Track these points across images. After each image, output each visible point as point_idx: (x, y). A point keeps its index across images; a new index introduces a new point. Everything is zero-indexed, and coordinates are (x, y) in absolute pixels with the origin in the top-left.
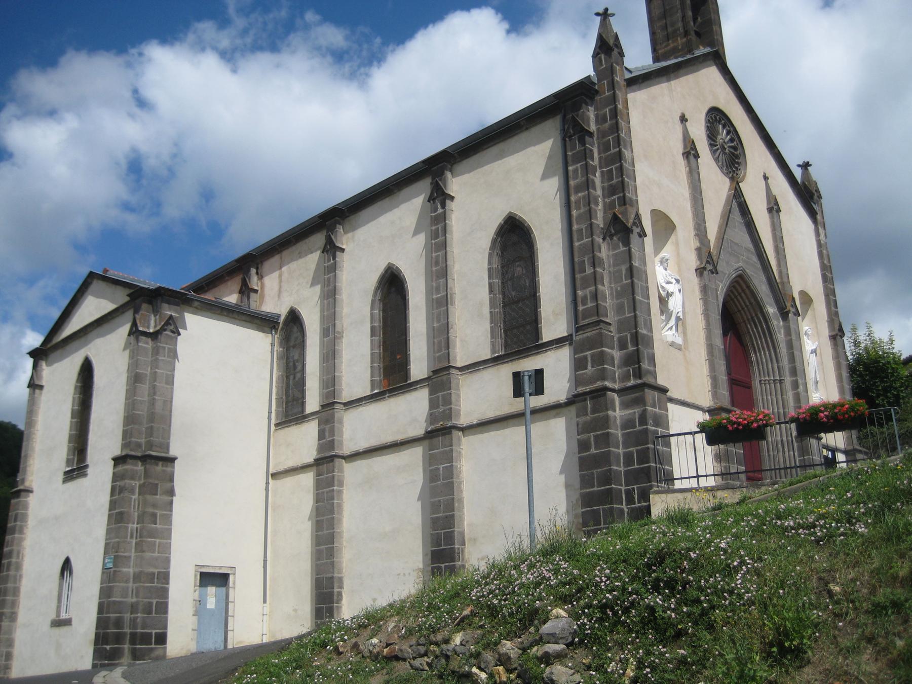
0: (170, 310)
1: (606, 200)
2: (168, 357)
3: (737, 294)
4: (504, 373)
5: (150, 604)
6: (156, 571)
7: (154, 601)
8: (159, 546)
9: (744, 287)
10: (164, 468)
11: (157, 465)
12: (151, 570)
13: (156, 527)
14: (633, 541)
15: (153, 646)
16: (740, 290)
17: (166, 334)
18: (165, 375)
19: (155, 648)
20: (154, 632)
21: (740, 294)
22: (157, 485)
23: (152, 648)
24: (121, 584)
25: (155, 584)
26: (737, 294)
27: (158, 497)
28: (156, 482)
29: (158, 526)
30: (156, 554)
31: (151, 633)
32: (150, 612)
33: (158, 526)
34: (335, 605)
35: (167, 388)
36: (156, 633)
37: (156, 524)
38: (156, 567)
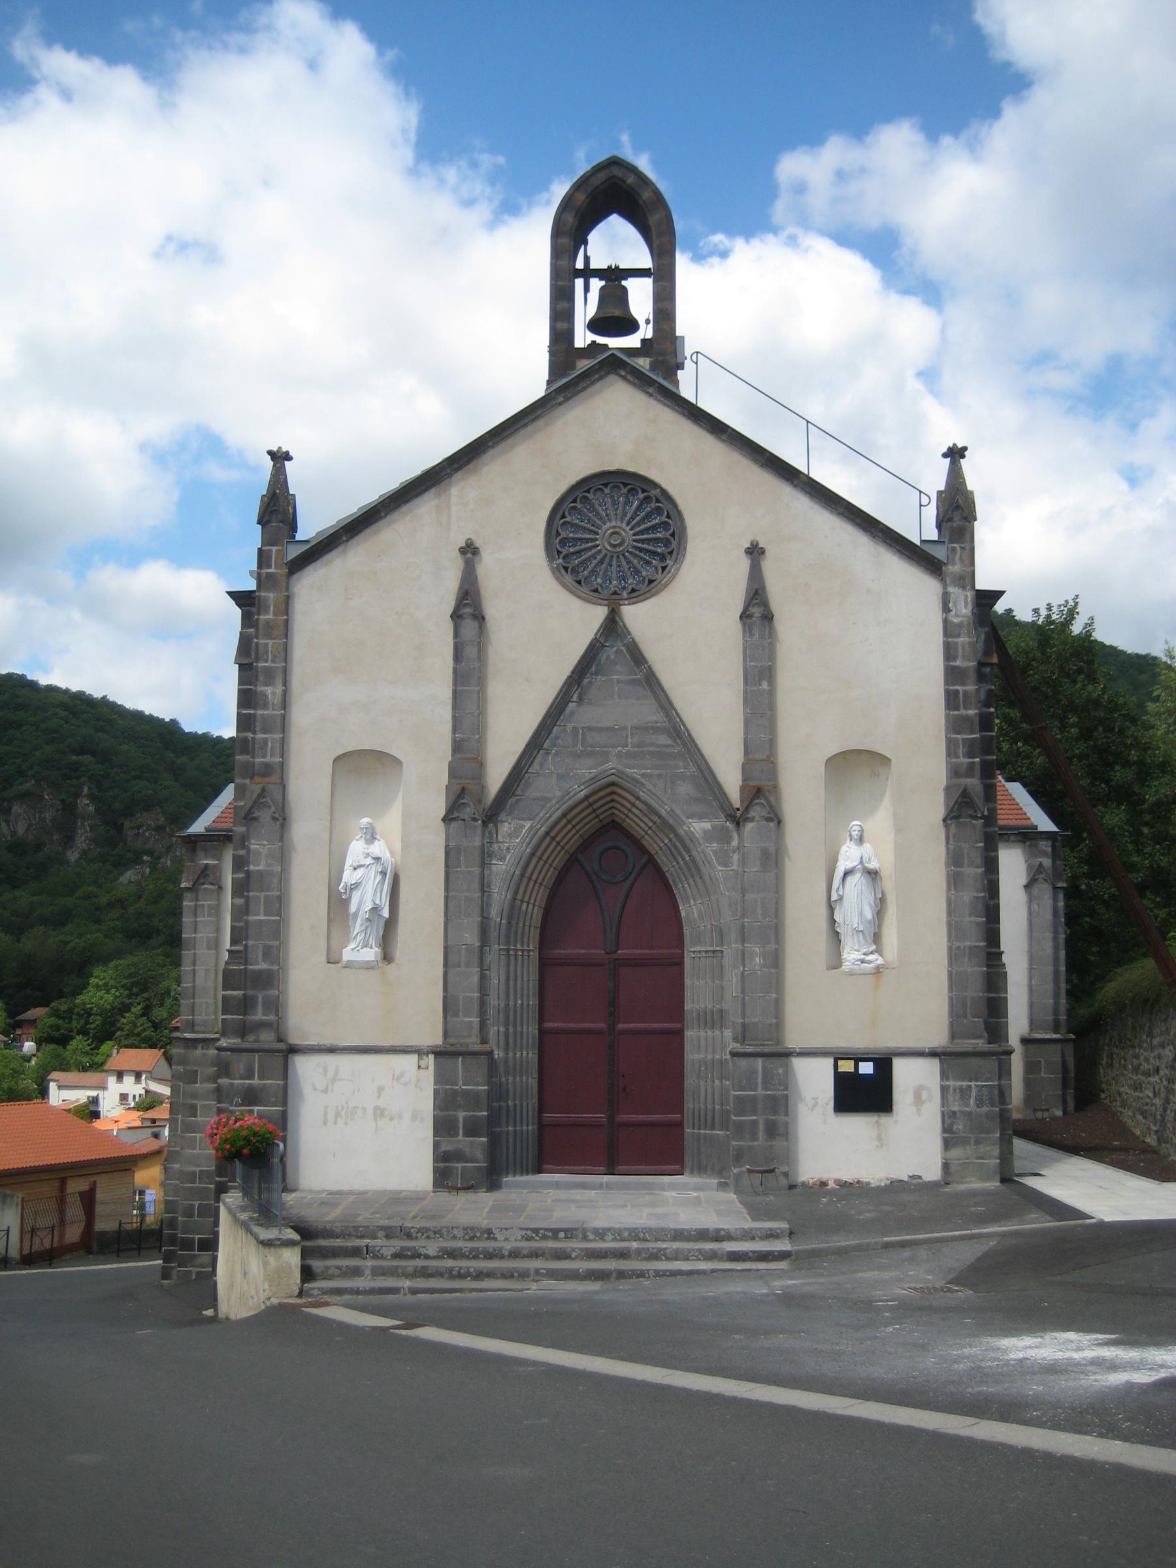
0: (206, 858)
1: (278, 759)
2: (209, 916)
3: (627, 812)
4: (150, 1131)
5: (192, 1207)
6: (197, 1169)
7: (197, 1204)
8: (200, 1142)
9: (632, 799)
10: (204, 1051)
11: (196, 1048)
12: (192, 1169)
13: (196, 1121)
14: (1164, 717)
15: (196, 1253)
16: (629, 806)
17: (205, 889)
18: (205, 938)
19: (199, 1255)
20: (197, 1237)
21: (633, 805)
22: (196, 1072)
23: (194, 1255)
24: (174, 1182)
25: (197, 1185)
26: (627, 812)
27: (198, 1085)
28: (196, 1068)
29: (199, 1119)
30: (197, 1151)
31: (194, 1238)
32: (191, 1216)
33: (199, 1119)
34: (972, 712)
35: (209, 954)
36: (199, 1238)
37: (196, 1117)
38: (199, 1166)
